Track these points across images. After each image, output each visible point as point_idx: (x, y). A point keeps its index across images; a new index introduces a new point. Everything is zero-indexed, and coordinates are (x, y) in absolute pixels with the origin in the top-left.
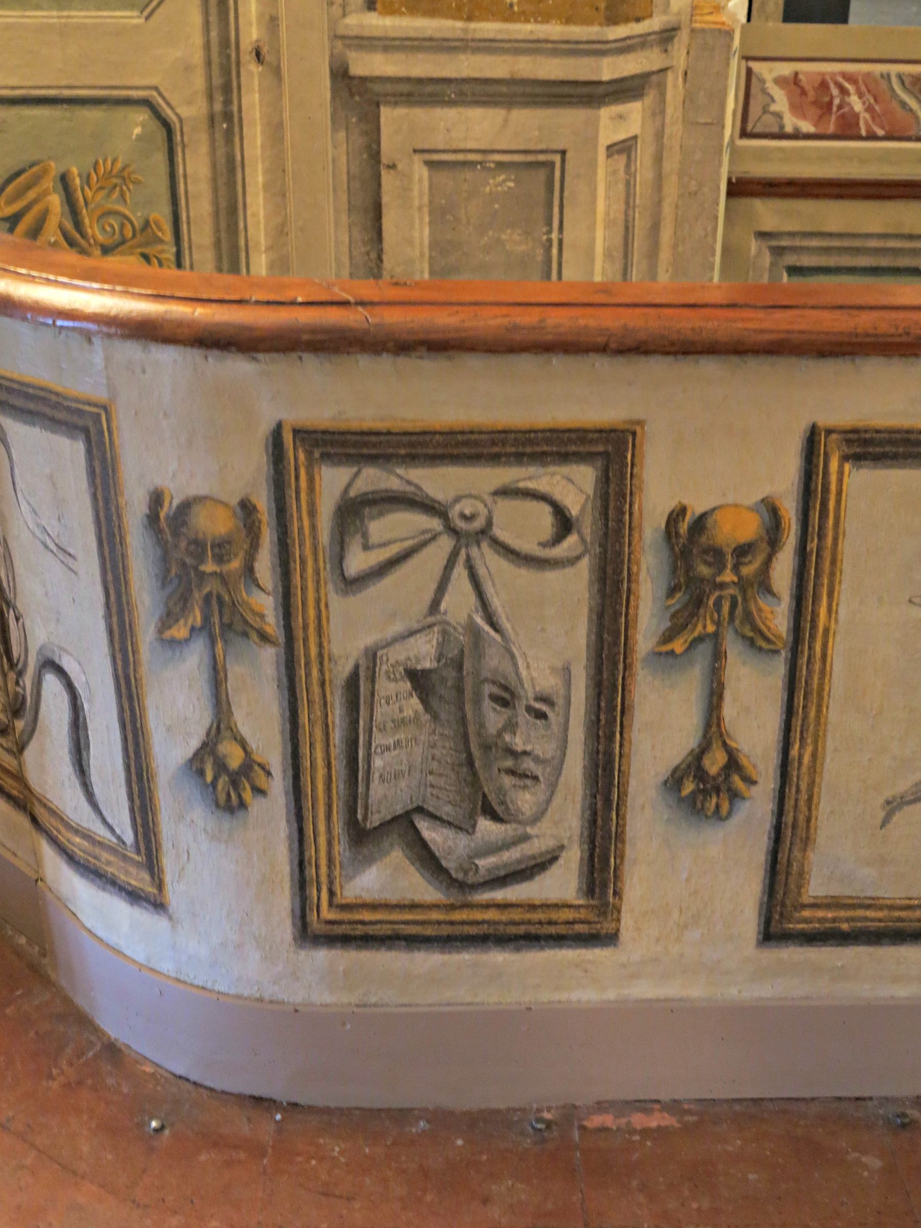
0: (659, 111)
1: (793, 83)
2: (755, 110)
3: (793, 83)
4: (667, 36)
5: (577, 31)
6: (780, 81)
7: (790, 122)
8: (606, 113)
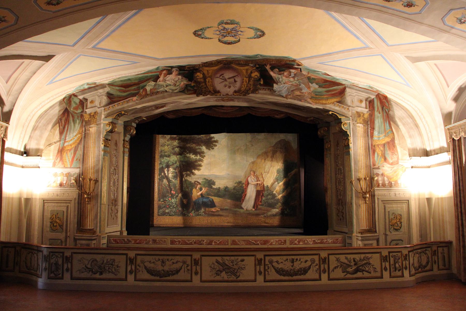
0: (97, 241)
1: (113, 239)
2: (110, 241)
3: (113, 239)
4: (97, 236)
5: (91, 235)
6: (112, 239)
7: (113, 242)
8: (93, 241)
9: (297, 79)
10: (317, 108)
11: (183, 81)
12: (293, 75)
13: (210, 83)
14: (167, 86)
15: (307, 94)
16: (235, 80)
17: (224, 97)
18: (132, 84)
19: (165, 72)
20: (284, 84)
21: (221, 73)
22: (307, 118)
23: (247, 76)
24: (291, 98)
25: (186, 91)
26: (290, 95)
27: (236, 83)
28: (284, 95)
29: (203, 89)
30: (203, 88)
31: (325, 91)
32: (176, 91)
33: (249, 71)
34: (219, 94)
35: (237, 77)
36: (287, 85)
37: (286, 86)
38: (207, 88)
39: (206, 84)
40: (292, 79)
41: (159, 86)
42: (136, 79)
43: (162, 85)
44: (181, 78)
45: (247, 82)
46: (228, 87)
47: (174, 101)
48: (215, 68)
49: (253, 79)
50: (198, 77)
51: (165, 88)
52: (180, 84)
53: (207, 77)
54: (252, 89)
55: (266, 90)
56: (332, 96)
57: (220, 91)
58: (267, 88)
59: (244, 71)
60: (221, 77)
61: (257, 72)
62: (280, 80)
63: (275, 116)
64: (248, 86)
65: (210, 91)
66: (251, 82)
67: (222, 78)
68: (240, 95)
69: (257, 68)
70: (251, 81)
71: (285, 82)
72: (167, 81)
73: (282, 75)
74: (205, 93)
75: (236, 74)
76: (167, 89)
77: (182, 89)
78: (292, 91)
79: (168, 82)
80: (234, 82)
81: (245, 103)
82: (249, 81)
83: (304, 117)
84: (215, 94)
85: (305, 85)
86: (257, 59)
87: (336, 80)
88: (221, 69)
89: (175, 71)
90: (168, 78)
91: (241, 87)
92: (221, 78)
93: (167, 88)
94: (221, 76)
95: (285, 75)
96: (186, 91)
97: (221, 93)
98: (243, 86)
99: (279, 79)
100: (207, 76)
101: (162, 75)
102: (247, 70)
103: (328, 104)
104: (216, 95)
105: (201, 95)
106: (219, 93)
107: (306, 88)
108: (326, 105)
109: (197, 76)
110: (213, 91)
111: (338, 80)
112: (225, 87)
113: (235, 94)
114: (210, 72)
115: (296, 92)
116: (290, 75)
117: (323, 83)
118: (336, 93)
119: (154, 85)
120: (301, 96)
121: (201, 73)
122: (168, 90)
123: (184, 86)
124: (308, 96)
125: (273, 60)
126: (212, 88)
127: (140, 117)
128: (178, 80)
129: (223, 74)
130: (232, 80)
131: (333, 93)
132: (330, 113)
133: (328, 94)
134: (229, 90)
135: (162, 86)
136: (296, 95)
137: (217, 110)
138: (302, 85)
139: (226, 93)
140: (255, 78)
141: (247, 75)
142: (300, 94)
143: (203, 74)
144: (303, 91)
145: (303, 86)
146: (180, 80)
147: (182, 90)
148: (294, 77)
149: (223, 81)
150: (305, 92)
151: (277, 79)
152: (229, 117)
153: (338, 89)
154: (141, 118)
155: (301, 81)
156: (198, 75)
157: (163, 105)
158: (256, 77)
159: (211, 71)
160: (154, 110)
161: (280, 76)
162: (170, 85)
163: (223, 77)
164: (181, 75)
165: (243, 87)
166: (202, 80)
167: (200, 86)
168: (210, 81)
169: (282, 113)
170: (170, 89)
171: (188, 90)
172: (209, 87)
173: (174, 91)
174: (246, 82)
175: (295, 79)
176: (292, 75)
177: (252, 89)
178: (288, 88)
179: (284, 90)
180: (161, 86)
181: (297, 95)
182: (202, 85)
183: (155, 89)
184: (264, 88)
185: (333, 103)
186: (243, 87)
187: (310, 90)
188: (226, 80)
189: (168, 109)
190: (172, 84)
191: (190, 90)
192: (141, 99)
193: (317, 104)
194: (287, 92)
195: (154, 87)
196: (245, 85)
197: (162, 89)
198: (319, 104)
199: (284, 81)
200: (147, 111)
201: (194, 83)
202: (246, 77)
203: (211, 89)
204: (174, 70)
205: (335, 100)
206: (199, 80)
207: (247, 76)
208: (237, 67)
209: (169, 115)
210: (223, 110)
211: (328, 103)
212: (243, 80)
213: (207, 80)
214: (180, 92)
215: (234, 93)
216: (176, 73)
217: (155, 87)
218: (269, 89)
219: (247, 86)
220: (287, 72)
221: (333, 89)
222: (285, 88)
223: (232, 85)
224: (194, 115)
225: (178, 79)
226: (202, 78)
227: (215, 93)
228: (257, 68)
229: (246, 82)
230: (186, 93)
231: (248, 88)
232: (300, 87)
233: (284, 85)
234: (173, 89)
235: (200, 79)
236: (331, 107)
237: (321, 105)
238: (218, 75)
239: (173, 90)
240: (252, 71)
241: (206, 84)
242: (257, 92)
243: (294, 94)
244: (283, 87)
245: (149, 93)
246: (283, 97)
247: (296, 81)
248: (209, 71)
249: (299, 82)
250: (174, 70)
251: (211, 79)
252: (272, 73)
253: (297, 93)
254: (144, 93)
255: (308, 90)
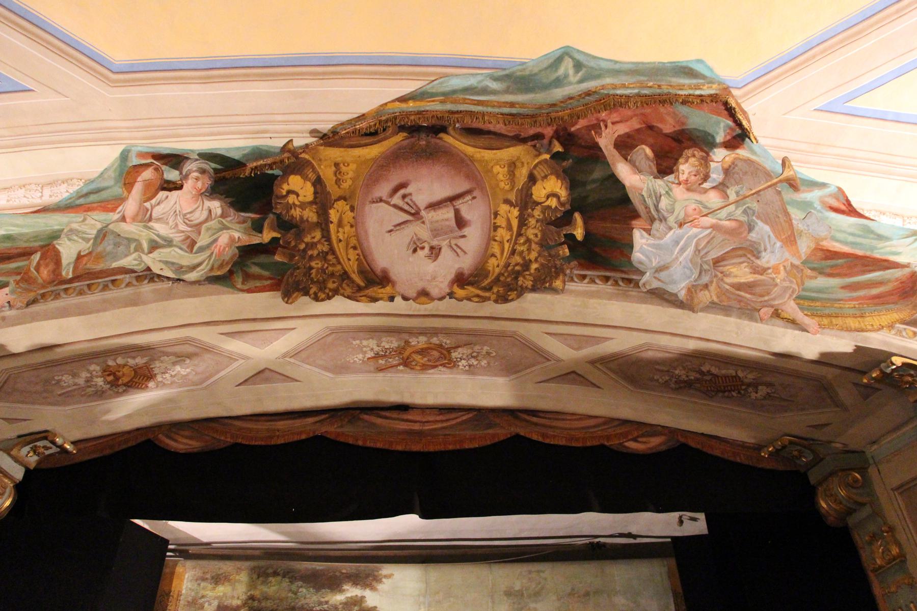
9: (737, 193)
10: (826, 360)
11: (228, 228)
12: (716, 176)
13: (347, 228)
14: (154, 246)
15: (783, 274)
16: (457, 213)
17: (410, 332)
18: (16, 251)
19: (148, 174)
20: (681, 225)
21: (396, 178)
22: (759, 448)
23: (512, 197)
24: (713, 303)
25: (240, 280)
26: (706, 286)
27: (466, 231)
28: (680, 288)
29: (313, 264)
30: (312, 256)
31: (843, 288)
32: (192, 276)
33: (522, 174)
34: (388, 289)
35: (469, 197)
36: (695, 230)
37: (690, 239)
38: (330, 257)
39: (327, 236)
40: (713, 199)
41: (117, 245)
42: (36, 237)
43: (130, 240)
44: (219, 211)
45: (515, 229)
46: (427, 251)
47: (186, 341)
48: (374, 151)
49: (537, 213)
50: (292, 199)
51: (144, 257)
52: (215, 240)
53: (333, 198)
54: (534, 266)
55: (593, 281)
56: (876, 305)
57: (393, 275)
58: (598, 277)
59: (501, 172)
60: (396, 200)
61: (558, 177)
62: (664, 203)
63: (626, 444)
64: (519, 248)
65: (345, 276)
66: (534, 232)
67: (400, 203)
68: (484, 299)
69: (556, 156)
70: (532, 222)
71: (682, 215)
72: (159, 220)
73: (671, 178)
74: (322, 286)
75: (464, 186)
76: (154, 262)
77: (221, 266)
78: (717, 262)
79: (161, 229)
80: (453, 223)
81: (501, 380)
82: (522, 222)
83: (743, 446)
84: (371, 291)
85: (772, 227)
86: (558, 94)
87: (875, 243)
88: (394, 158)
89: (196, 174)
90: (162, 206)
91: (486, 255)
92: (395, 206)
93: (155, 254)
94: (396, 190)
95: (683, 177)
96: (238, 279)
97: (393, 284)
98: (496, 249)
99: (658, 198)
100: (333, 189)
101: (138, 188)
102: (512, 166)
103: (870, 331)
104: (374, 300)
105: (306, 293)
106: (384, 287)
107: (778, 244)
108: (865, 334)
109: (289, 192)
110: (362, 272)
111: (881, 244)
112: (415, 251)
113: (460, 292)
114: (349, 171)
115: (734, 270)
116: (706, 178)
117: (823, 262)
118: (890, 293)
119: (96, 238)
120: (758, 290)
121: (305, 178)
122: (156, 270)
123: (230, 253)
124: (787, 284)
125: (628, 97)
126: (352, 254)
127: (45, 435)
128: (206, 221)
129: (403, 186)
130: (446, 215)
131: (875, 291)
132: (898, 361)
133: (855, 294)
134: (430, 267)
135: (133, 246)
136: (733, 285)
137: (379, 421)
138: (760, 223)
139: (420, 285)
140: (549, 207)
141: (512, 189)
142: (750, 278)
143: (318, 183)
144: (768, 259)
145: (763, 229)
146: (213, 224)
147: (219, 273)
148: (721, 187)
149: (407, 217)
150: (773, 263)
151: (650, 202)
152: (431, 449)
153: (889, 281)
154: (46, 438)
155: (755, 205)
156: (292, 187)
157: (140, 361)
158: (553, 202)
159: (353, 166)
160: (100, 395)
161: (659, 182)
162: (169, 243)
163: (404, 197)
164: (220, 199)
165: (493, 255)
166: (310, 215)
167: (302, 246)
168: (345, 221)
169: (652, 430)
170: (166, 263)
171: (247, 277)
172: (340, 249)
173: (186, 272)
174: (509, 228)
175: (726, 196)
176: (713, 176)
177: (534, 266)
178: (697, 251)
179: (681, 259)
180: (128, 247)
181: (739, 287)
182: (308, 239)
183: (100, 257)
184: (584, 277)
185: (891, 327)
186: (493, 255)
187: (796, 253)
188: (416, 215)
189: (169, 400)
190: (177, 238)
191: (259, 277)
192: (34, 302)
193: (825, 331)
194: (695, 275)
195: (94, 244)
196: (507, 245)
197: (128, 261)
198: (833, 332)
199: (679, 212)
200: (67, 397)
201: (272, 228)
202: (507, 201)
203: (352, 266)
204: (190, 172)
205: (895, 316)
206: (296, 213)
207: (512, 197)
208: (470, 150)
209: (176, 441)
210: (407, 421)
211: (869, 327)
212: (496, 214)
213: (333, 215)
214: (213, 280)
215: (456, 289)
216: (199, 185)
217: (100, 249)
218: (606, 279)
219: (513, 252)
220: (692, 160)
221: (870, 280)
222: (683, 250)
223: (444, 244)
224: (281, 441)
225: (205, 214)
226: (311, 203)
227: (366, 287)
228: (556, 156)
229: (509, 228)
230: (239, 286)
231: (517, 259)
232: (753, 236)
233: (679, 231)
234: (182, 267)
235: (303, 206)
236: (887, 339)
237: (845, 334)
238: (383, 190)
239: (180, 269)
240: (535, 172)
241: (328, 231)
242: (558, 283)
243: (728, 280)
244: (677, 243)
245: (67, 272)
246: (673, 302)
247: (732, 207)
248: (344, 169)
249: (745, 212)
250: (190, 172)
251: (352, 209)
252: (624, 171)
253: (740, 273)
254: (45, 273)
255: (787, 255)
